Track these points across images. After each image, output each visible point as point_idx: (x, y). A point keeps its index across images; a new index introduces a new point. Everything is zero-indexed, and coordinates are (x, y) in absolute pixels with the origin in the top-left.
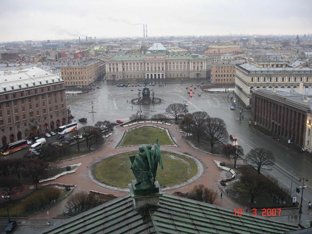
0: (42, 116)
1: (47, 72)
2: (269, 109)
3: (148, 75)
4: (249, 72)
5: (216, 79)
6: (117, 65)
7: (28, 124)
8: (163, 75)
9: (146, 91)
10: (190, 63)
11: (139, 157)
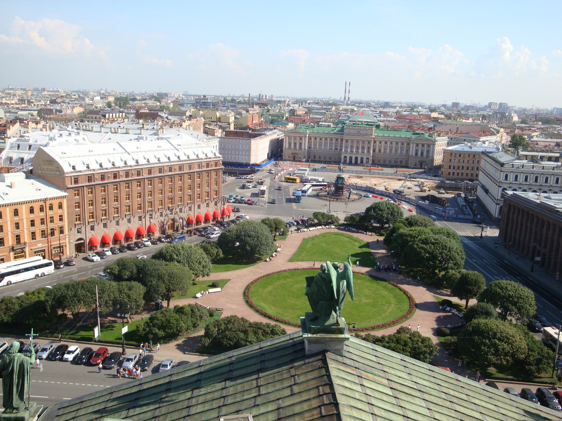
0: (186, 204)
1: (198, 142)
2: (529, 225)
3: (345, 157)
4: (502, 165)
6: (301, 139)
7: (164, 213)
8: (368, 158)
10: (411, 145)
11: (320, 279)
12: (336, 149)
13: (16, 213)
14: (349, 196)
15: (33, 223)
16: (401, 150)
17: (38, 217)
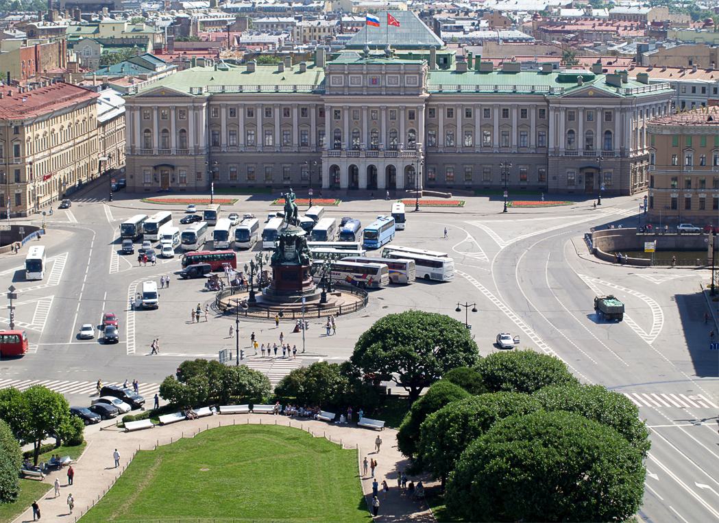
3: (334, 169)
5: (674, 200)
8: (409, 169)
9: (290, 252)
10: (551, 113)
12: (304, 145)
14: (324, 300)
16: (521, 135)
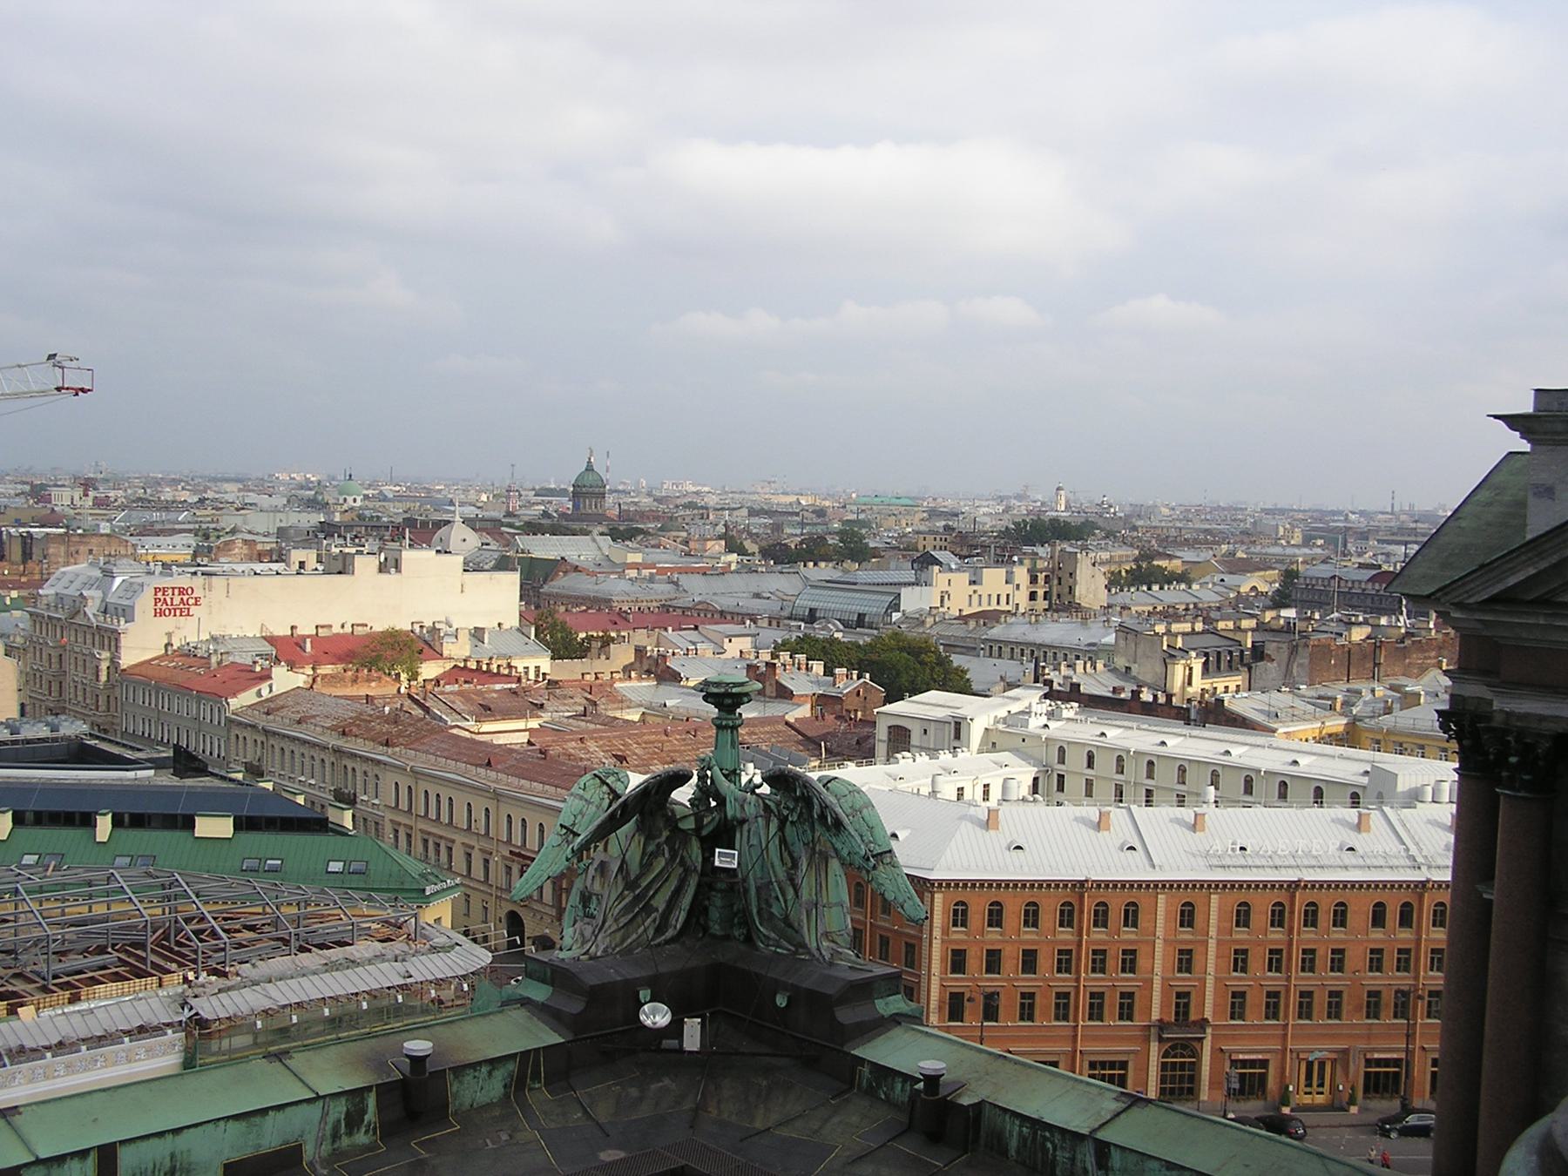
13: (1187, 916)
15: (1240, 960)
17: (1260, 943)
